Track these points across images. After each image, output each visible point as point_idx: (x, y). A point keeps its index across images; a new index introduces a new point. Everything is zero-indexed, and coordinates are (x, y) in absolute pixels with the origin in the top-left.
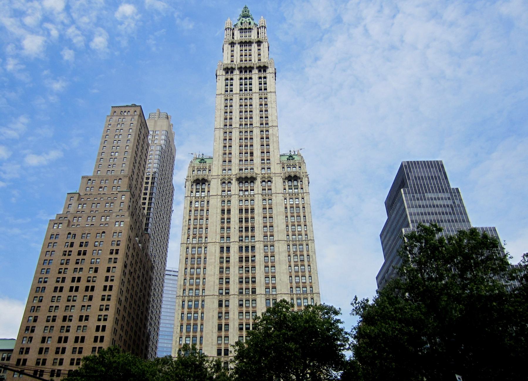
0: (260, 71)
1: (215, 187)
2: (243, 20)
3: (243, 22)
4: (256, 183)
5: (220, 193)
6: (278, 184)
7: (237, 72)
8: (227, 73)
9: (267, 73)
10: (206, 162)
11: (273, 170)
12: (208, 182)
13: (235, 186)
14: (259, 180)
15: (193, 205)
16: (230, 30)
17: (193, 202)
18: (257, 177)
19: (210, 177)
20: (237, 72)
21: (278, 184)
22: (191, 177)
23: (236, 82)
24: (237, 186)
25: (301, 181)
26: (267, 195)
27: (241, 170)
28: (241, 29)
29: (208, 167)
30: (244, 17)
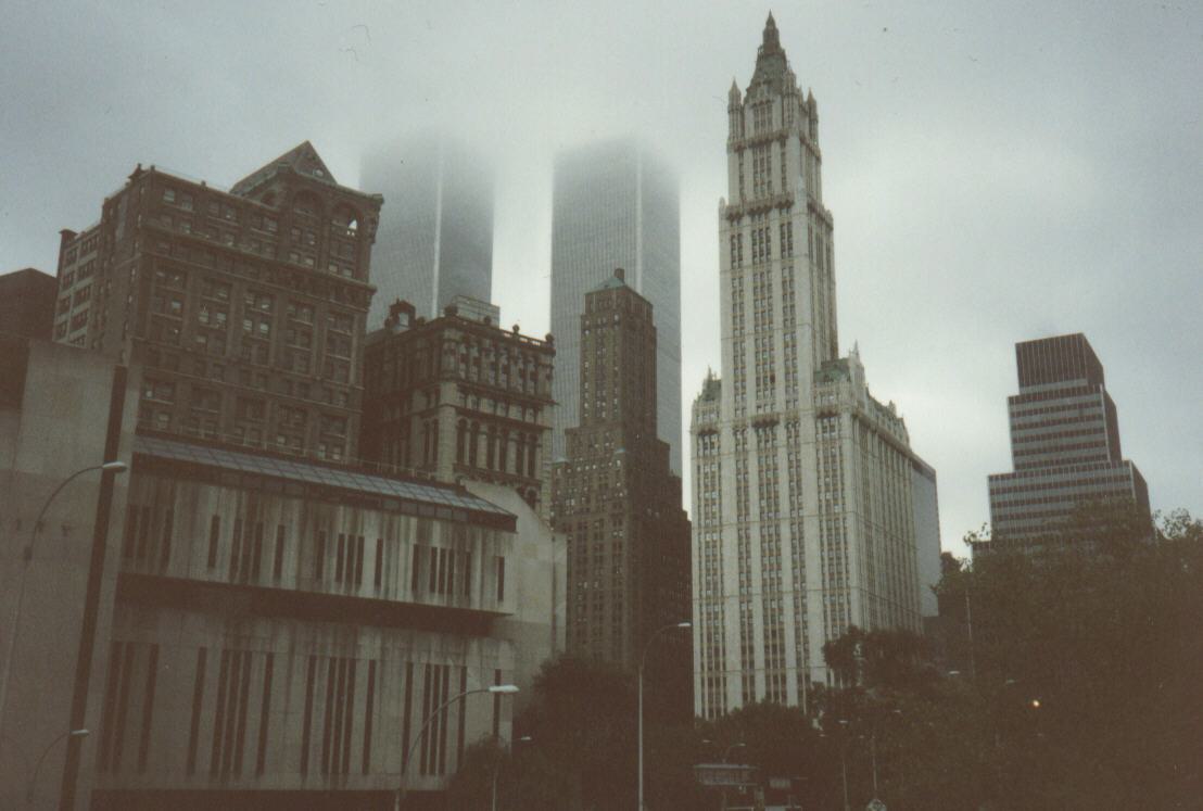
1: (726, 440)
5: (733, 450)
6: (808, 427)
7: (746, 220)
13: (751, 434)
14: (782, 424)
15: (702, 471)
17: (702, 467)
18: (778, 418)
19: (719, 426)
20: (746, 220)
21: (808, 427)
23: (747, 242)
24: (754, 435)
26: (794, 447)
27: (759, 407)
28: (755, 105)
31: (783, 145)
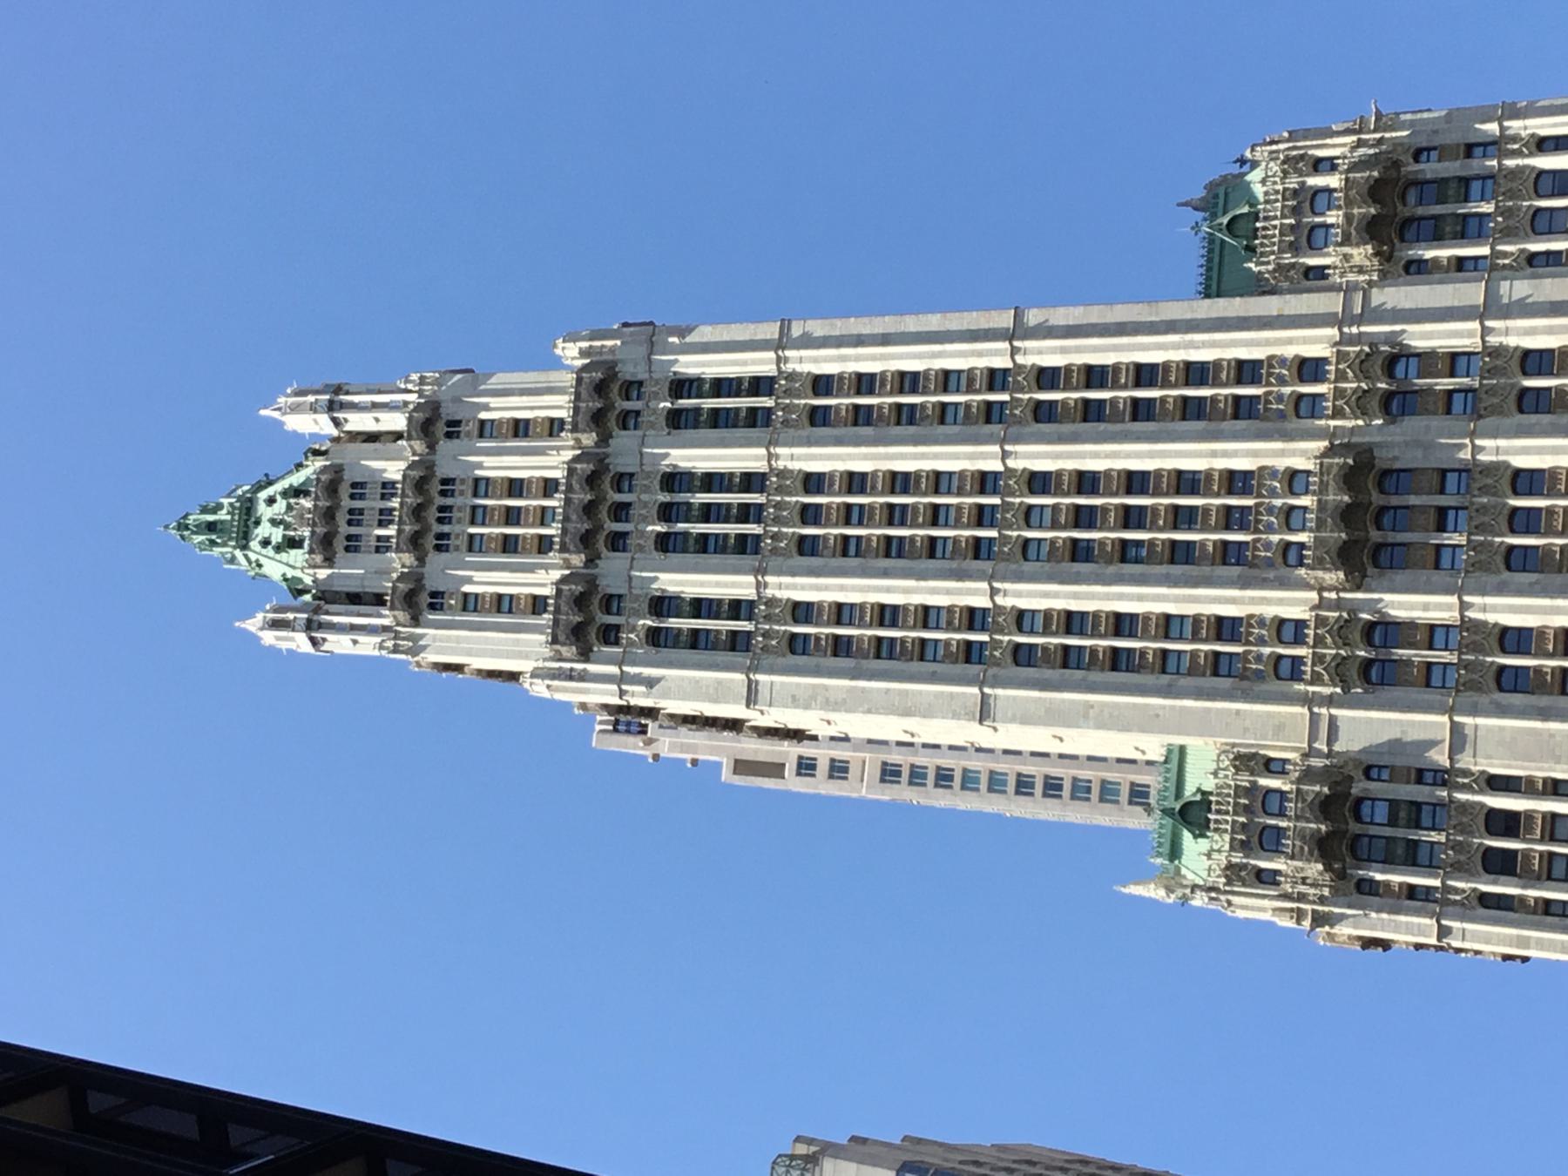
0: (628, 420)
2: (266, 543)
3: (277, 535)
4: (1396, 452)
7: (612, 570)
8: (610, 635)
9: (640, 377)
10: (1204, 793)
11: (1316, 344)
12: (1351, 779)
16: (327, 613)
20: (612, 570)
22: (1302, 897)
25: (1417, 155)
29: (1244, 780)
30: (244, 541)
31: (454, 429)
